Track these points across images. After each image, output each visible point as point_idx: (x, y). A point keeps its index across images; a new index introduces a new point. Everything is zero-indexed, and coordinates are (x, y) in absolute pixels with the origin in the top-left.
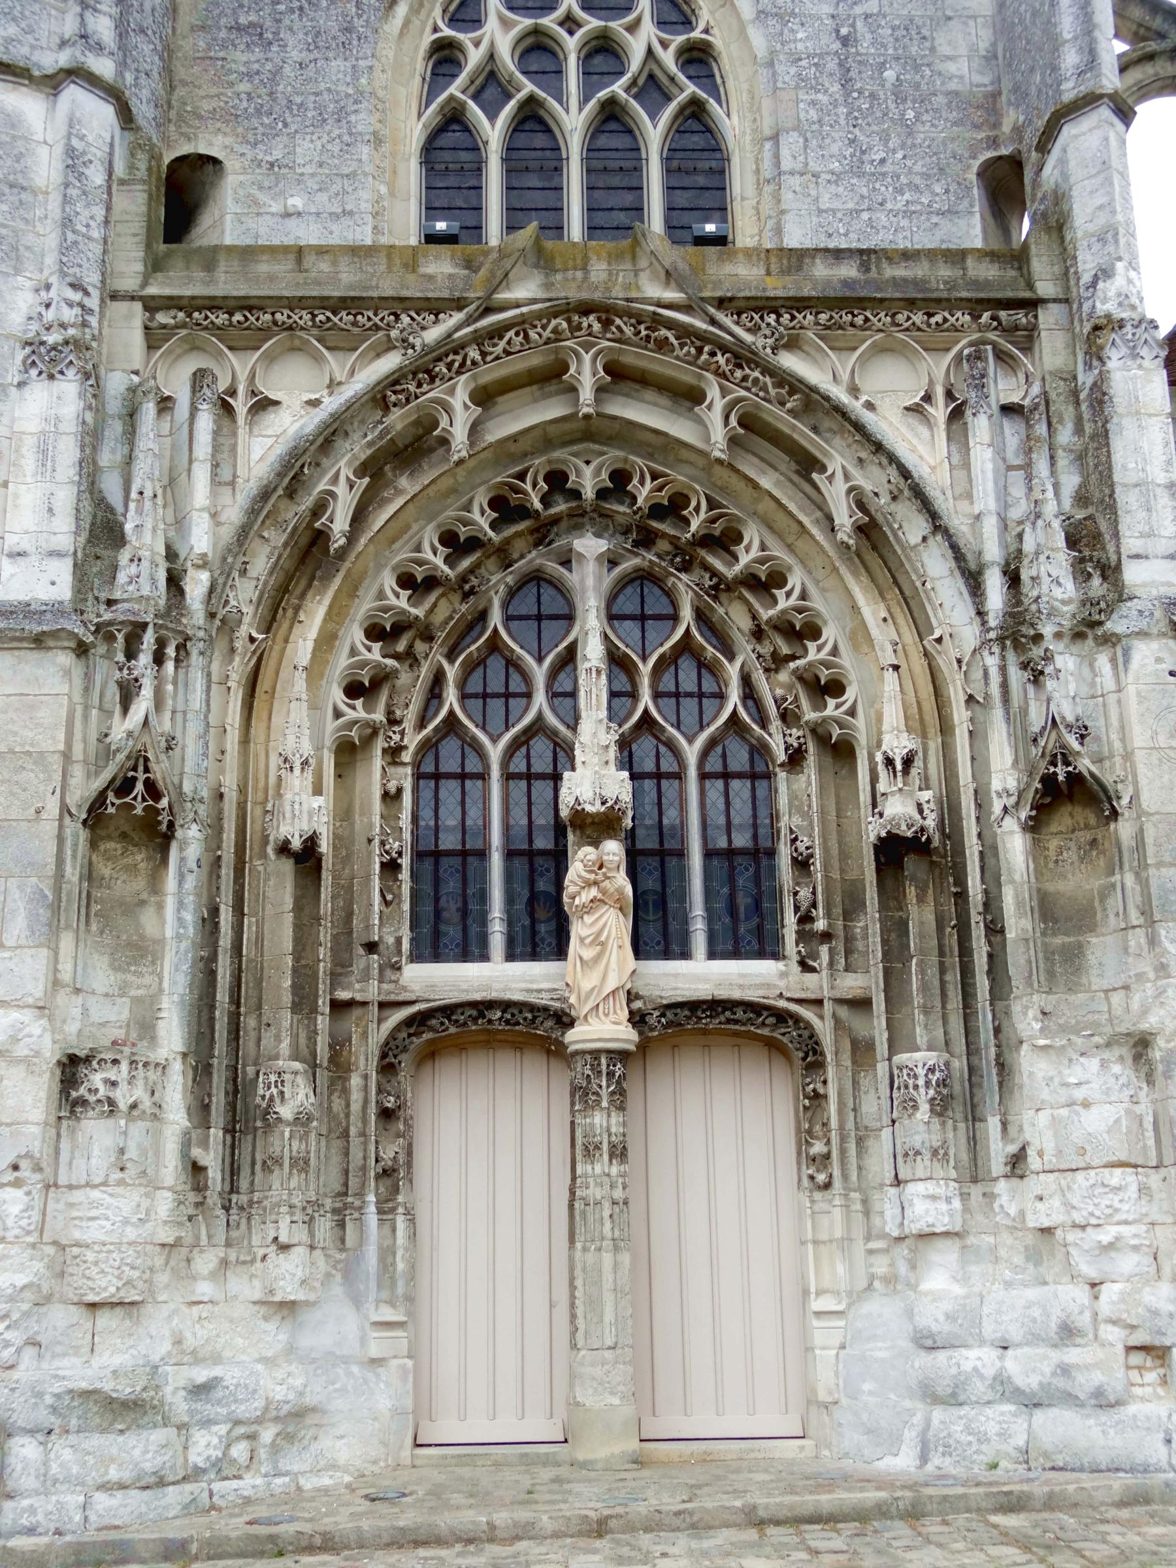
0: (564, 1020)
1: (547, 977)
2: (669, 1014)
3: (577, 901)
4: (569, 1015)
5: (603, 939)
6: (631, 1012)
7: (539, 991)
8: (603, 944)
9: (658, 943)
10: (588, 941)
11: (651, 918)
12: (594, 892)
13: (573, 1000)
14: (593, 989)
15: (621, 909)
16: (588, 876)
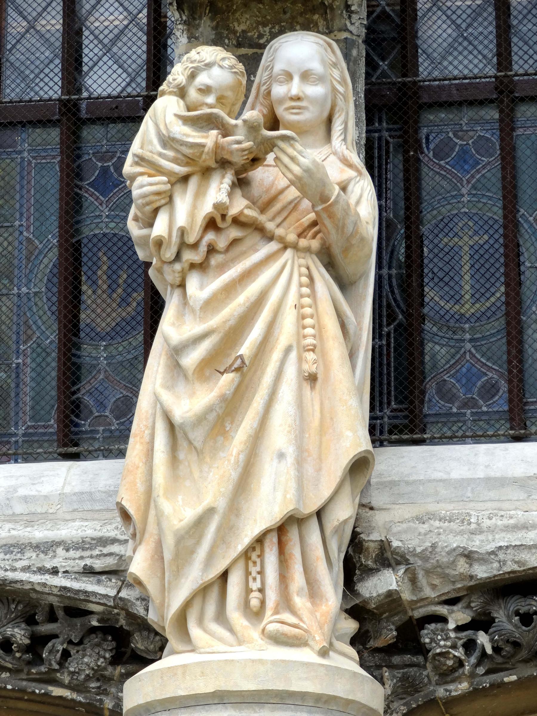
0: (130, 640)
1: (82, 504)
2: (504, 617)
3: (160, 228)
4: (144, 626)
5: (246, 348)
6: (356, 611)
7: (47, 547)
8: (246, 372)
9: (490, 390)
10: (191, 359)
11: (468, 308)
12: (217, 190)
13: (139, 566)
14: (200, 523)
15: (330, 263)
16: (193, 136)
